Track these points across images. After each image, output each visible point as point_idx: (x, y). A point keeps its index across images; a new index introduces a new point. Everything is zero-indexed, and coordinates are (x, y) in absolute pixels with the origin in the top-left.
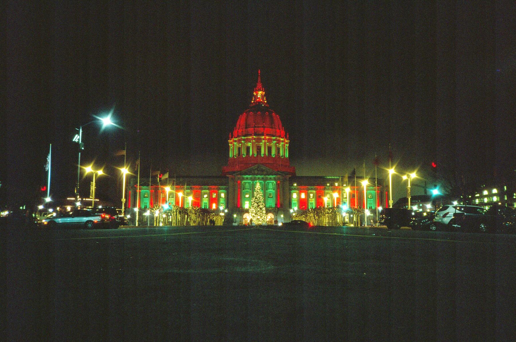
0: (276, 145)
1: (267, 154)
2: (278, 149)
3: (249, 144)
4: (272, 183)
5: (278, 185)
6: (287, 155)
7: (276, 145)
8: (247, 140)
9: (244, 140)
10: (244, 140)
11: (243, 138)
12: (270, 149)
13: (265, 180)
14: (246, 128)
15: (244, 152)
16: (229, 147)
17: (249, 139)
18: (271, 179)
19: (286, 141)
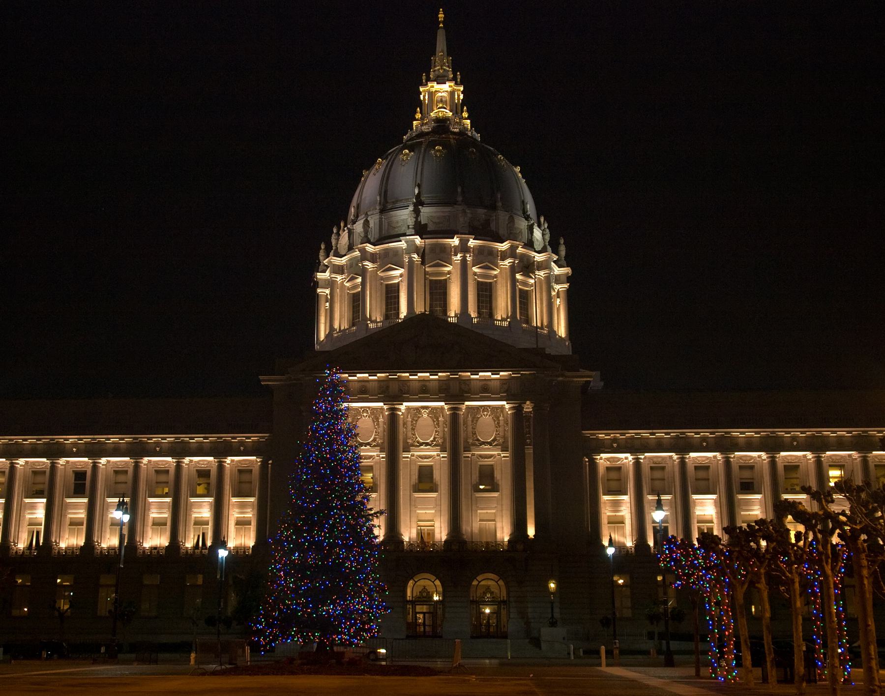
0: (514, 281)
1: (473, 312)
2: (522, 299)
3: (397, 274)
6: (561, 329)
7: (514, 281)
8: (390, 259)
9: (373, 258)
10: (373, 258)
11: (370, 248)
12: (486, 293)
13: (454, 393)
14: (383, 211)
15: (374, 312)
17: (396, 252)
18: (485, 390)
19: (557, 270)
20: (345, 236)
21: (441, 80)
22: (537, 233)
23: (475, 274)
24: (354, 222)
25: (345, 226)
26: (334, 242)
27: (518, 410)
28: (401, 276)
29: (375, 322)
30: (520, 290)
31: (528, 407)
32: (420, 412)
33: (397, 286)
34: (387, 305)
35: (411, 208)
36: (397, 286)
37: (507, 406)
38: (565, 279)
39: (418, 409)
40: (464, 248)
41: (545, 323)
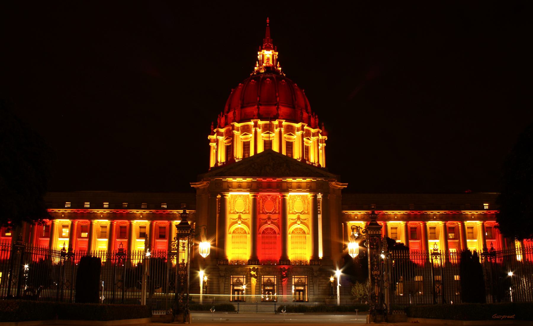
0: (303, 141)
2: (306, 150)
4: (304, 198)
5: (315, 201)
6: (322, 163)
8: (246, 130)
11: (237, 125)
12: (290, 145)
14: (242, 107)
15: (239, 154)
16: (209, 148)
18: (299, 187)
19: (320, 137)
20: (223, 120)
21: (268, 49)
22: (312, 121)
23: (285, 138)
24: (228, 112)
25: (223, 114)
26: (219, 121)
27: (315, 197)
28: (251, 138)
29: (239, 159)
30: (306, 146)
31: (320, 196)
32: (267, 198)
33: (249, 142)
34: (244, 150)
35: (256, 107)
36: (249, 142)
37: (309, 195)
38: (324, 141)
39: (265, 196)
40: (280, 125)
41: (316, 161)
